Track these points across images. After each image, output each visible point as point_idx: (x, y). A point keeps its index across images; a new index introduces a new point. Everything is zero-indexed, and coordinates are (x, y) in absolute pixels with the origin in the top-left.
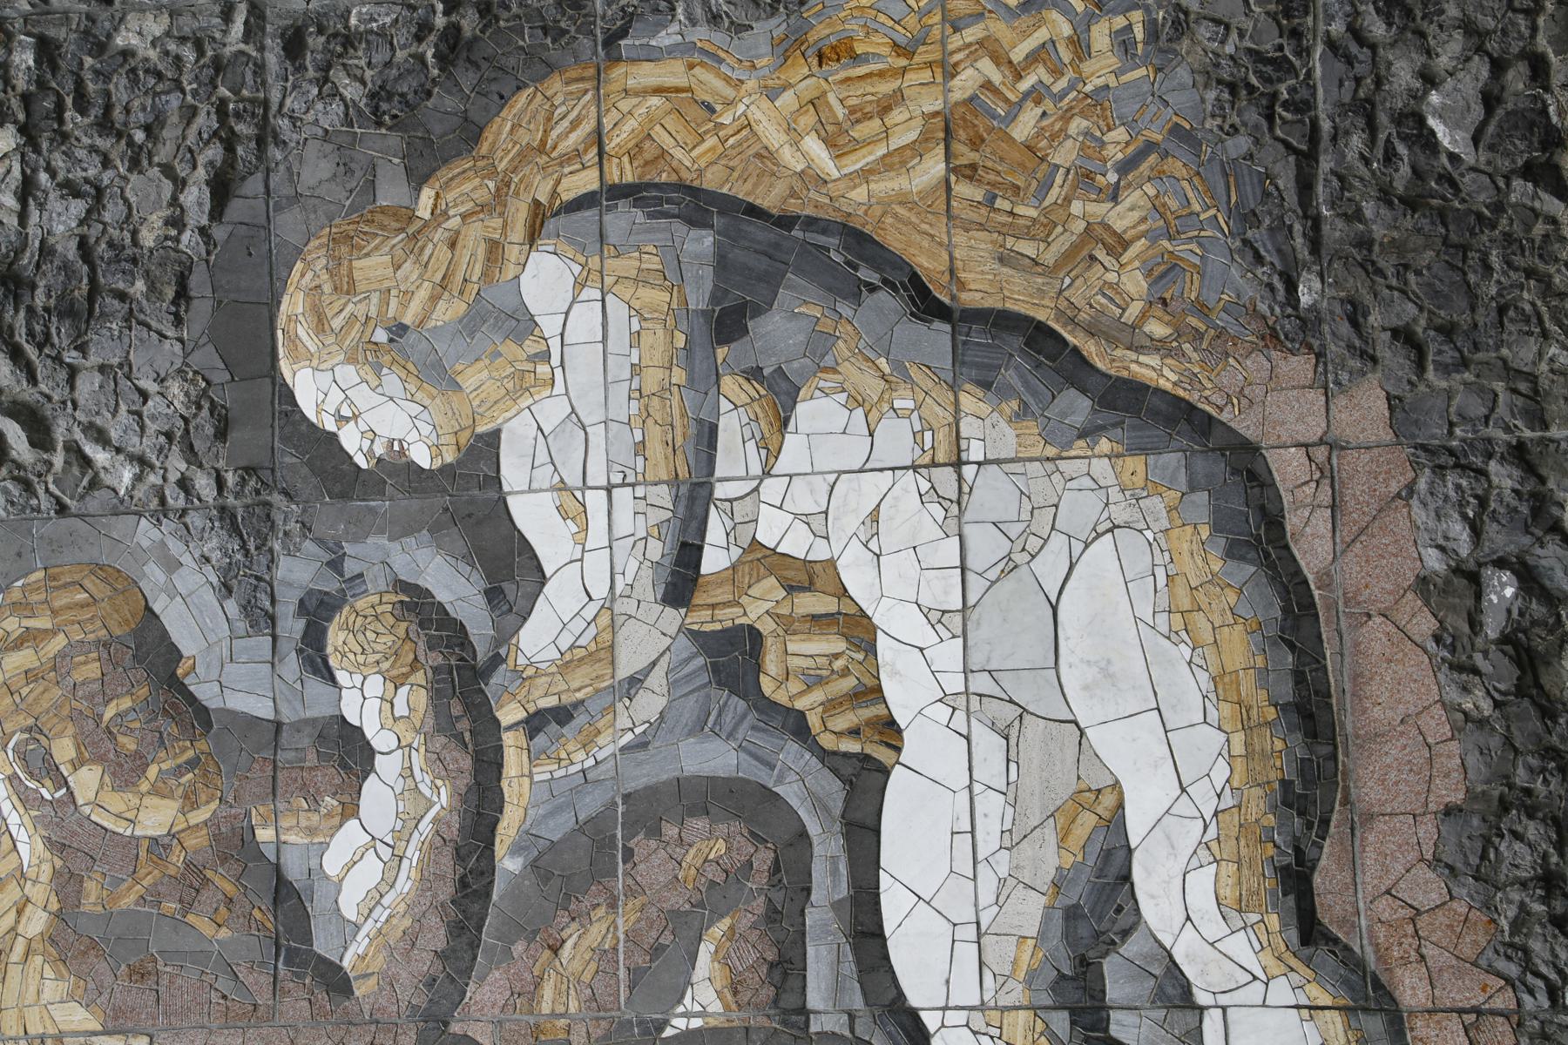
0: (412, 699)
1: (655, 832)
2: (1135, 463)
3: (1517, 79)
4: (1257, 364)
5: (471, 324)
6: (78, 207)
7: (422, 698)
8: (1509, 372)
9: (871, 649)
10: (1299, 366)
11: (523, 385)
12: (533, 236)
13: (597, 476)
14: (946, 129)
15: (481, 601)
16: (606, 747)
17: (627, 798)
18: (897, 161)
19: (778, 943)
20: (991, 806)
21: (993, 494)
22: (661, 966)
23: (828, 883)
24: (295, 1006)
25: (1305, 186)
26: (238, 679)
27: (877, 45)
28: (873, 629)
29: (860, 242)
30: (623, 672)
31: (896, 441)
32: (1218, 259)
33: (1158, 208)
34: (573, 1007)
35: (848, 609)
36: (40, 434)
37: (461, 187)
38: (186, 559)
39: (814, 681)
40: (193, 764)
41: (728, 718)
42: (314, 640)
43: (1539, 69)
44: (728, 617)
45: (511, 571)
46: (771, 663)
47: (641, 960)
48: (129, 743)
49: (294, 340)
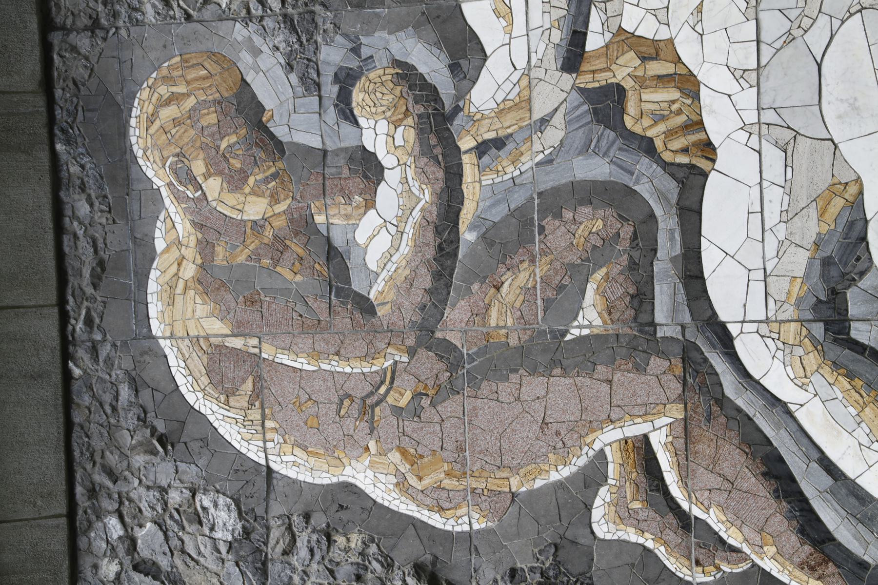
0: (406, 135)
1: (558, 216)
7: (412, 134)
9: (696, 97)
15: (446, 72)
16: (527, 163)
17: (540, 194)
19: (636, 283)
20: (775, 197)
22: (564, 296)
23: (668, 245)
24: (343, 321)
26: (300, 124)
28: (698, 83)
30: (537, 115)
34: (510, 322)
35: (681, 71)
38: (265, 48)
39: (659, 118)
40: (275, 176)
41: (604, 144)
44: (604, 79)
45: (466, 53)
46: (631, 107)
47: (550, 294)
48: (237, 164)
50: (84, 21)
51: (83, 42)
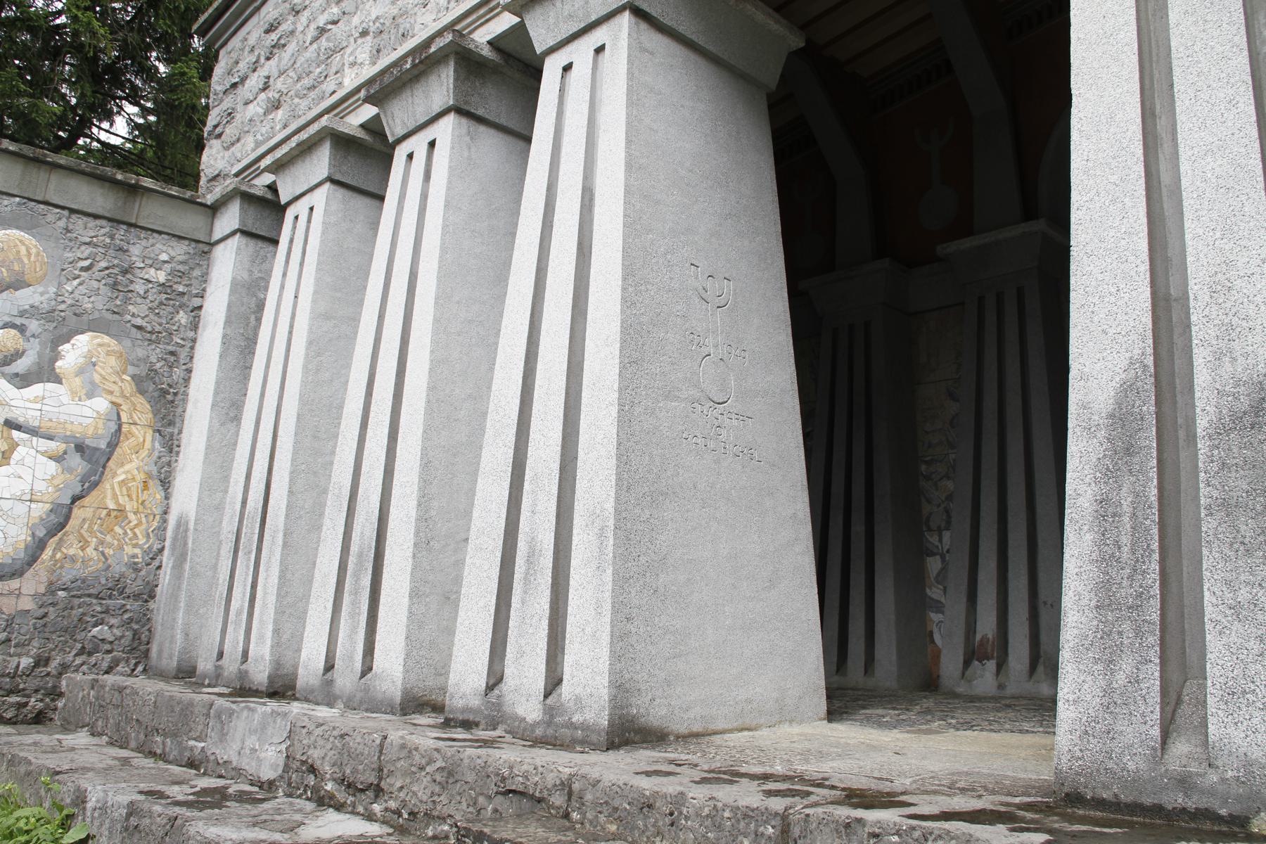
2: (23, 546)
3: (108, 647)
4: (45, 579)
5: (92, 383)
6: (142, 292)
8: (31, 640)
10: (42, 589)
11: (73, 393)
12: (113, 403)
13: (45, 408)
14: (121, 510)
18: (115, 496)
21: (21, 509)
25: (89, 596)
27: (145, 496)
29: (95, 485)
31: (40, 486)
32: (74, 573)
33: (90, 560)
36: (82, 269)
37: (128, 386)
42: (14, 326)
43: (109, 652)
45: (23, 381)
49: (97, 337)
50: (71, 227)
51: (62, 223)
